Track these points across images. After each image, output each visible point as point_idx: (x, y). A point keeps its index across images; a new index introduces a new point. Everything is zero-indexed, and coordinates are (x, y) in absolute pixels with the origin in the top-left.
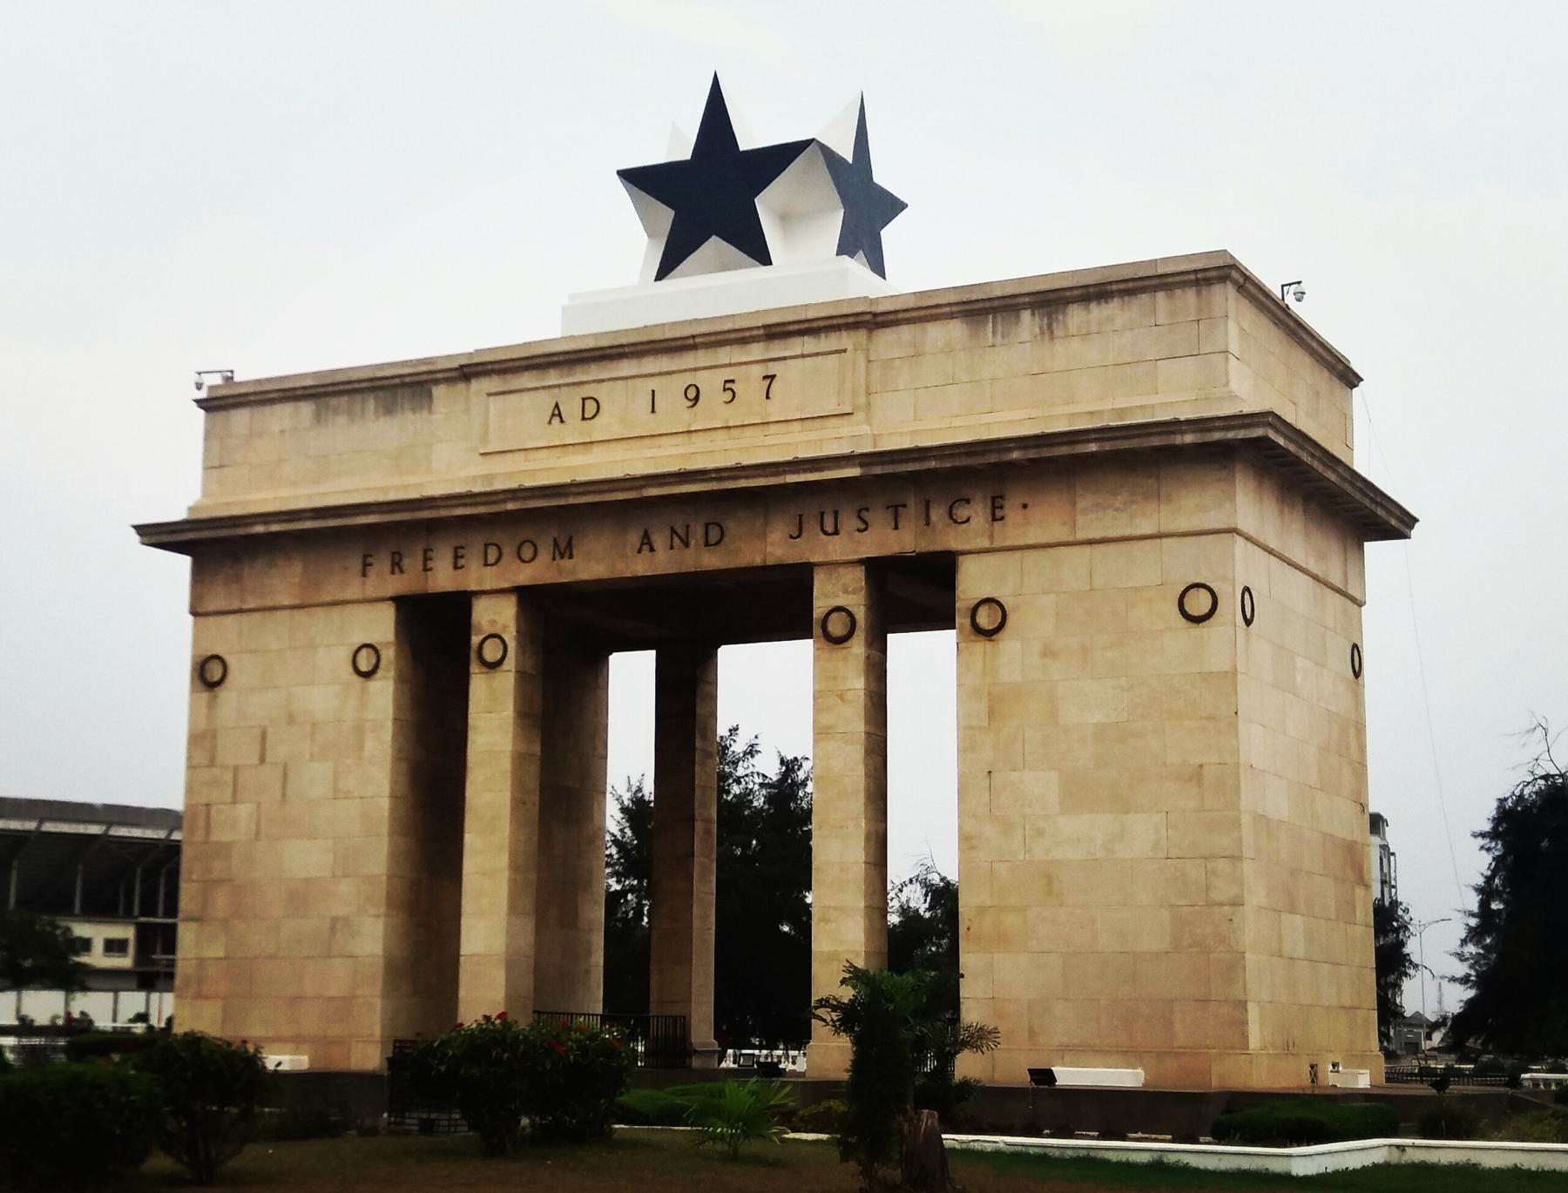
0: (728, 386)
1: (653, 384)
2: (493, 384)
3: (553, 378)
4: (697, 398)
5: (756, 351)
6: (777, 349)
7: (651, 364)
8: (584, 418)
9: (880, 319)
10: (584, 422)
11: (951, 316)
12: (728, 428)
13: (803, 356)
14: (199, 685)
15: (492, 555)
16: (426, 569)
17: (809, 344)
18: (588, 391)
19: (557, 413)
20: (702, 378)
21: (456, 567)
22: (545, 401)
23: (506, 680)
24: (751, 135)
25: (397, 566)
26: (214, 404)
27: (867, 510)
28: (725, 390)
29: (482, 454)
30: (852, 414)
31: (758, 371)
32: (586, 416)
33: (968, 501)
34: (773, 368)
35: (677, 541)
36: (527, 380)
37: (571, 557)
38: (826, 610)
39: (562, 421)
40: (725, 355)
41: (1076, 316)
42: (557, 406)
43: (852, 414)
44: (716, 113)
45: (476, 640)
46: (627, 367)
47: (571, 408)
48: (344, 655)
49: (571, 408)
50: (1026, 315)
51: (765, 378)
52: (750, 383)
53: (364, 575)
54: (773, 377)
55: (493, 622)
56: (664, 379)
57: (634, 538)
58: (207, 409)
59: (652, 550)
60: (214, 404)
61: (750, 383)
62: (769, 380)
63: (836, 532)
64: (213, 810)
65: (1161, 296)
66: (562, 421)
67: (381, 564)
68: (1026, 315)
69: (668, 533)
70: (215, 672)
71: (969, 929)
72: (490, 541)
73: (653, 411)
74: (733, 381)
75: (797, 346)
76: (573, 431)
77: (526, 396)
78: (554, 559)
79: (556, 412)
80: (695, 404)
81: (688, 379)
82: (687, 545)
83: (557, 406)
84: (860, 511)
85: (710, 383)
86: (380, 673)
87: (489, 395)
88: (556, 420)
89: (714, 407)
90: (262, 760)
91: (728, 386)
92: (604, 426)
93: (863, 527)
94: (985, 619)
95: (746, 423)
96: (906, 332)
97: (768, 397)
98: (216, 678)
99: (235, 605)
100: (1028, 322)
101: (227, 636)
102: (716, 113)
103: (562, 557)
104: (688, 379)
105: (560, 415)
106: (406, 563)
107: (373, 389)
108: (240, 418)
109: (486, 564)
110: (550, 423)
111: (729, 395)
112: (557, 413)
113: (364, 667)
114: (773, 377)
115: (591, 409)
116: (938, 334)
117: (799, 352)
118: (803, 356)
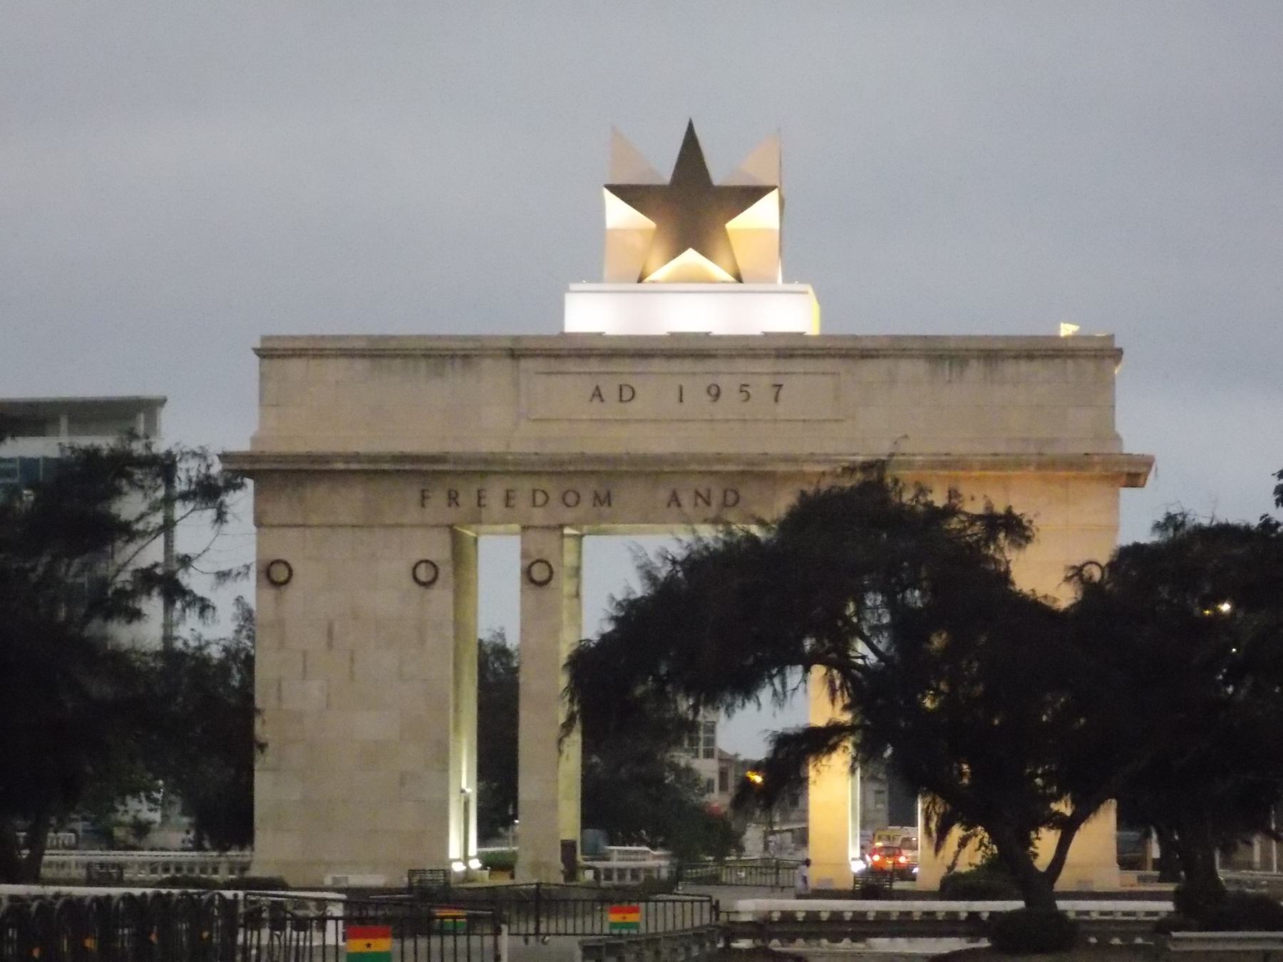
0: (745, 388)
2: (540, 364)
3: (594, 365)
4: (718, 395)
5: (767, 366)
6: (783, 365)
7: (676, 365)
8: (621, 400)
10: (622, 405)
11: (918, 357)
13: (805, 373)
14: (266, 582)
15: (540, 498)
16: (479, 505)
17: (810, 365)
19: (598, 394)
21: (507, 505)
22: (587, 386)
25: (453, 499)
26: (266, 353)
28: (741, 391)
30: (842, 420)
31: (766, 381)
32: (624, 399)
34: (779, 380)
35: (700, 500)
36: (571, 365)
37: (610, 504)
39: (602, 401)
40: (741, 365)
41: (1009, 368)
42: (597, 388)
43: (842, 420)
46: (657, 365)
47: (610, 390)
48: (404, 568)
49: (610, 390)
50: (974, 363)
51: (775, 386)
52: (761, 388)
53: (423, 505)
54: (780, 386)
57: (663, 494)
58: (258, 355)
59: (679, 505)
60: (266, 353)
61: (761, 388)
62: (778, 388)
65: (1070, 363)
66: (602, 401)
67: (438, 497)
68: (973, 363)
69: (692, 494)
70: (280, 573)
72: (537, 487)
73: (681, 401)
75: (797, 365)
76: (612, 408)
78: (594, 505)
79: (597, 393)
81: (710, 380)
82: (708, 503)
83: (597, 388)
86: (439, 583)
88: (596, 400)
90: (330, 645)
92: (635, 408)
97: (776, 400)
98: (282, 579)
99: (299, 520)
100: (975, 370)
101: (288, 546)
103: (601, 504)
105: (600, 395)
106: (461, 499)
107: (427, 356)
108: (295, 367)
109: (534, 506)
110: (591, 401)
112: (598, 394)
114: (780, 386)
115: (626, 394)
116: (908, 368)
117: (802, 370)
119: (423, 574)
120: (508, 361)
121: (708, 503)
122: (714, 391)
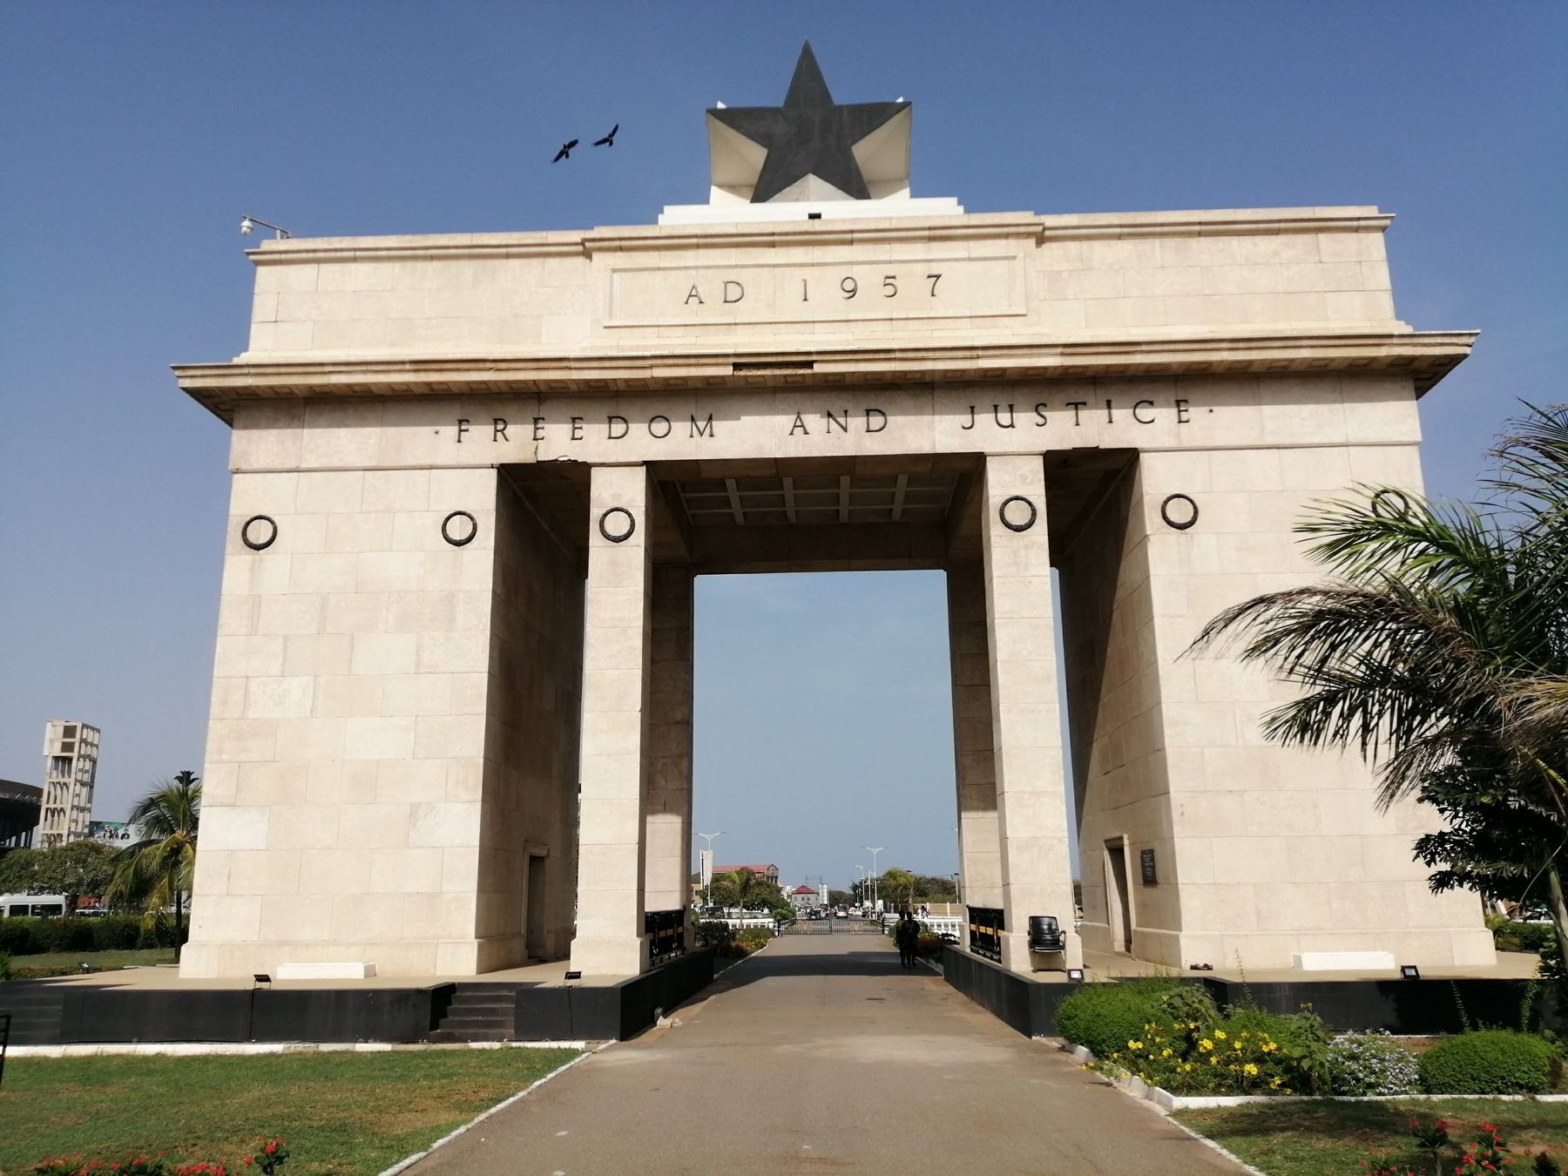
0: (888, 281)
1: (807, 273)
2: (619, 259)
4: (854, 291)
5: (918, 251)
9: (1047, 233)
12: (891, 319)
13: (970, 259)
16: (535, 439)
18: (733, 275)
20: (857, 272)
22: (683, 282)
23: (635, 553)
24: (844, 93)
27: (1045, 405)
28: (885, 285)
29: (605, 327)
33: (1151, 403)
34: (935, 269)
38: (1003, 500)
44: (808, 72)
45: (595, 512)
49: (711, 287)
51: (929, 277)
52: (912, 281)
54: (938, 277)
55: (616, 496)
56: (816, 271)
61: (912, 281)
63: (1012, 426)
64: (253, 685)
71: (1182, 814)
74: (894, 277)
77: (659, 275)
80: (852, 297)
81: (844, 272)
82: (845, 430)
84: (1037, 406)
85: (869, 279)
87: (615, 271)
89: (872, 299)
91: (888, 281)
92: (742, 312)
93: (1041, 421)
94: (1179, 512)
95: (911, 316)
96: (1073, 246)
102: (808, 72)
104: (844, 272)
111: (890, 290)
113: (456, 535)
114: (938, 277)
118: (970, 259)
119: (458, 529)
120: (581, 260)
121: (845, 430)
122: (849, 285)
